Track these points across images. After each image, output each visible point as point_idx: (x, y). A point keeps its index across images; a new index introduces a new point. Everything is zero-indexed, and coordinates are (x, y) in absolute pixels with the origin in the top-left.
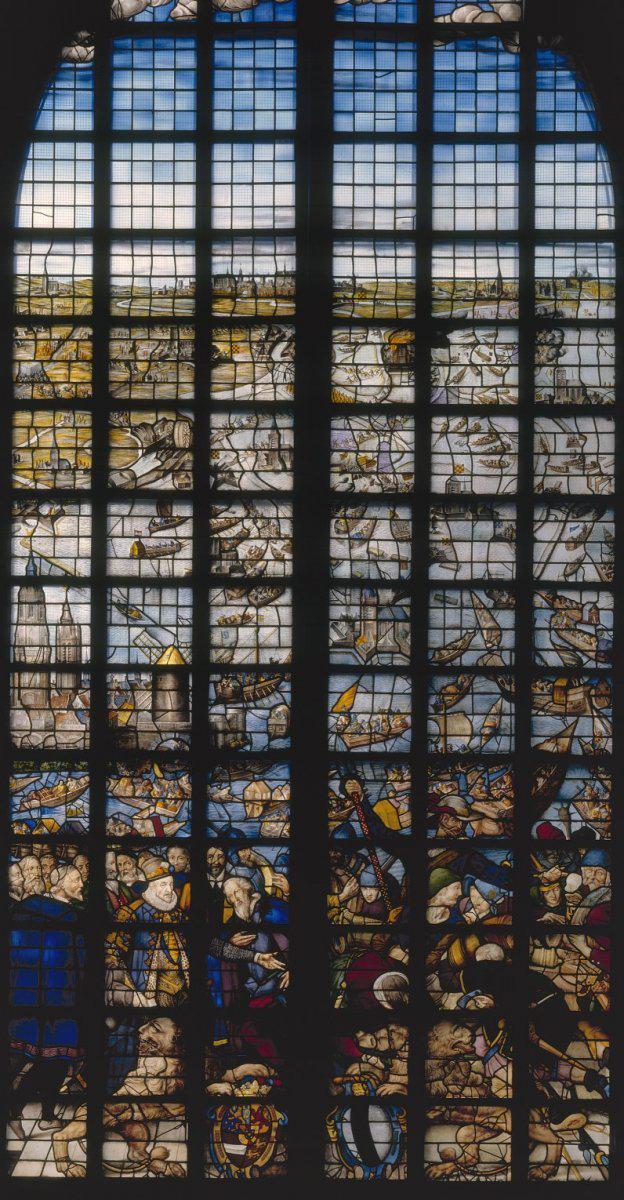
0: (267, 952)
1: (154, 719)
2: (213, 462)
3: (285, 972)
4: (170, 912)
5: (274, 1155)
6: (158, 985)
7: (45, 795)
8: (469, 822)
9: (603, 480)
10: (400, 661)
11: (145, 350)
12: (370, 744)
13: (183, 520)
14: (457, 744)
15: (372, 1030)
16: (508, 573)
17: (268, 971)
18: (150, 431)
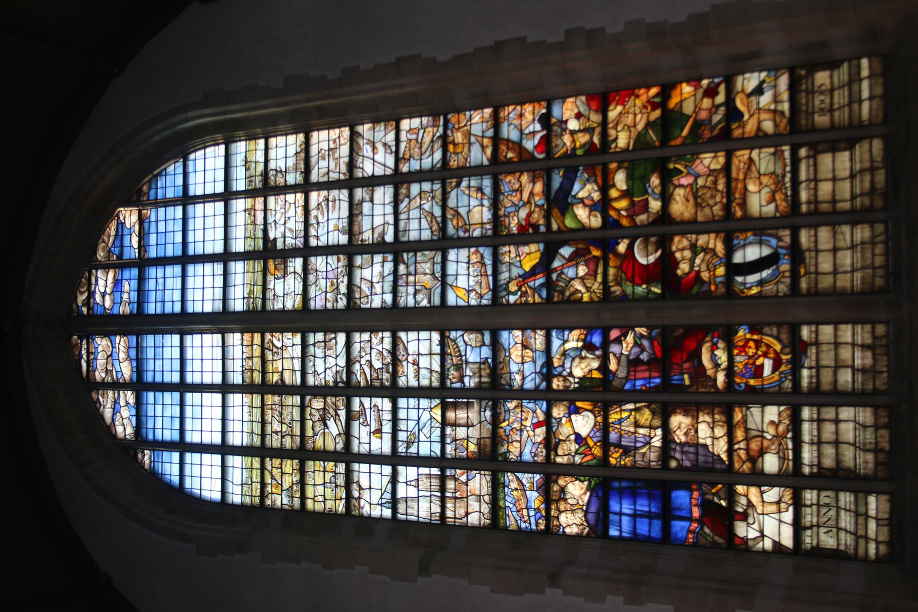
0: (622, 344)
1: (473, 426)
2: (331, 384)
3: (635, 331)
4: (596, 417)
5: (771, 336)
6: (647, 428)
7: (520, 505)
8: (535, 203)
9: (343, 135)
10: (438, 258)
11: (276, 426)
12: (487, 275)
13: (361, 404)
14: (487, 215)
15: (676, 264)
16: (390, 190)
17: (636, 344)
18: (315, 424)
